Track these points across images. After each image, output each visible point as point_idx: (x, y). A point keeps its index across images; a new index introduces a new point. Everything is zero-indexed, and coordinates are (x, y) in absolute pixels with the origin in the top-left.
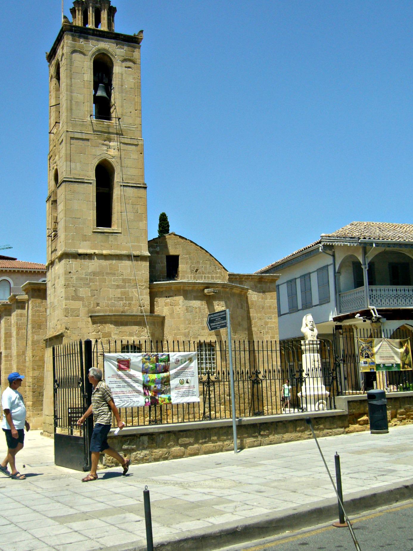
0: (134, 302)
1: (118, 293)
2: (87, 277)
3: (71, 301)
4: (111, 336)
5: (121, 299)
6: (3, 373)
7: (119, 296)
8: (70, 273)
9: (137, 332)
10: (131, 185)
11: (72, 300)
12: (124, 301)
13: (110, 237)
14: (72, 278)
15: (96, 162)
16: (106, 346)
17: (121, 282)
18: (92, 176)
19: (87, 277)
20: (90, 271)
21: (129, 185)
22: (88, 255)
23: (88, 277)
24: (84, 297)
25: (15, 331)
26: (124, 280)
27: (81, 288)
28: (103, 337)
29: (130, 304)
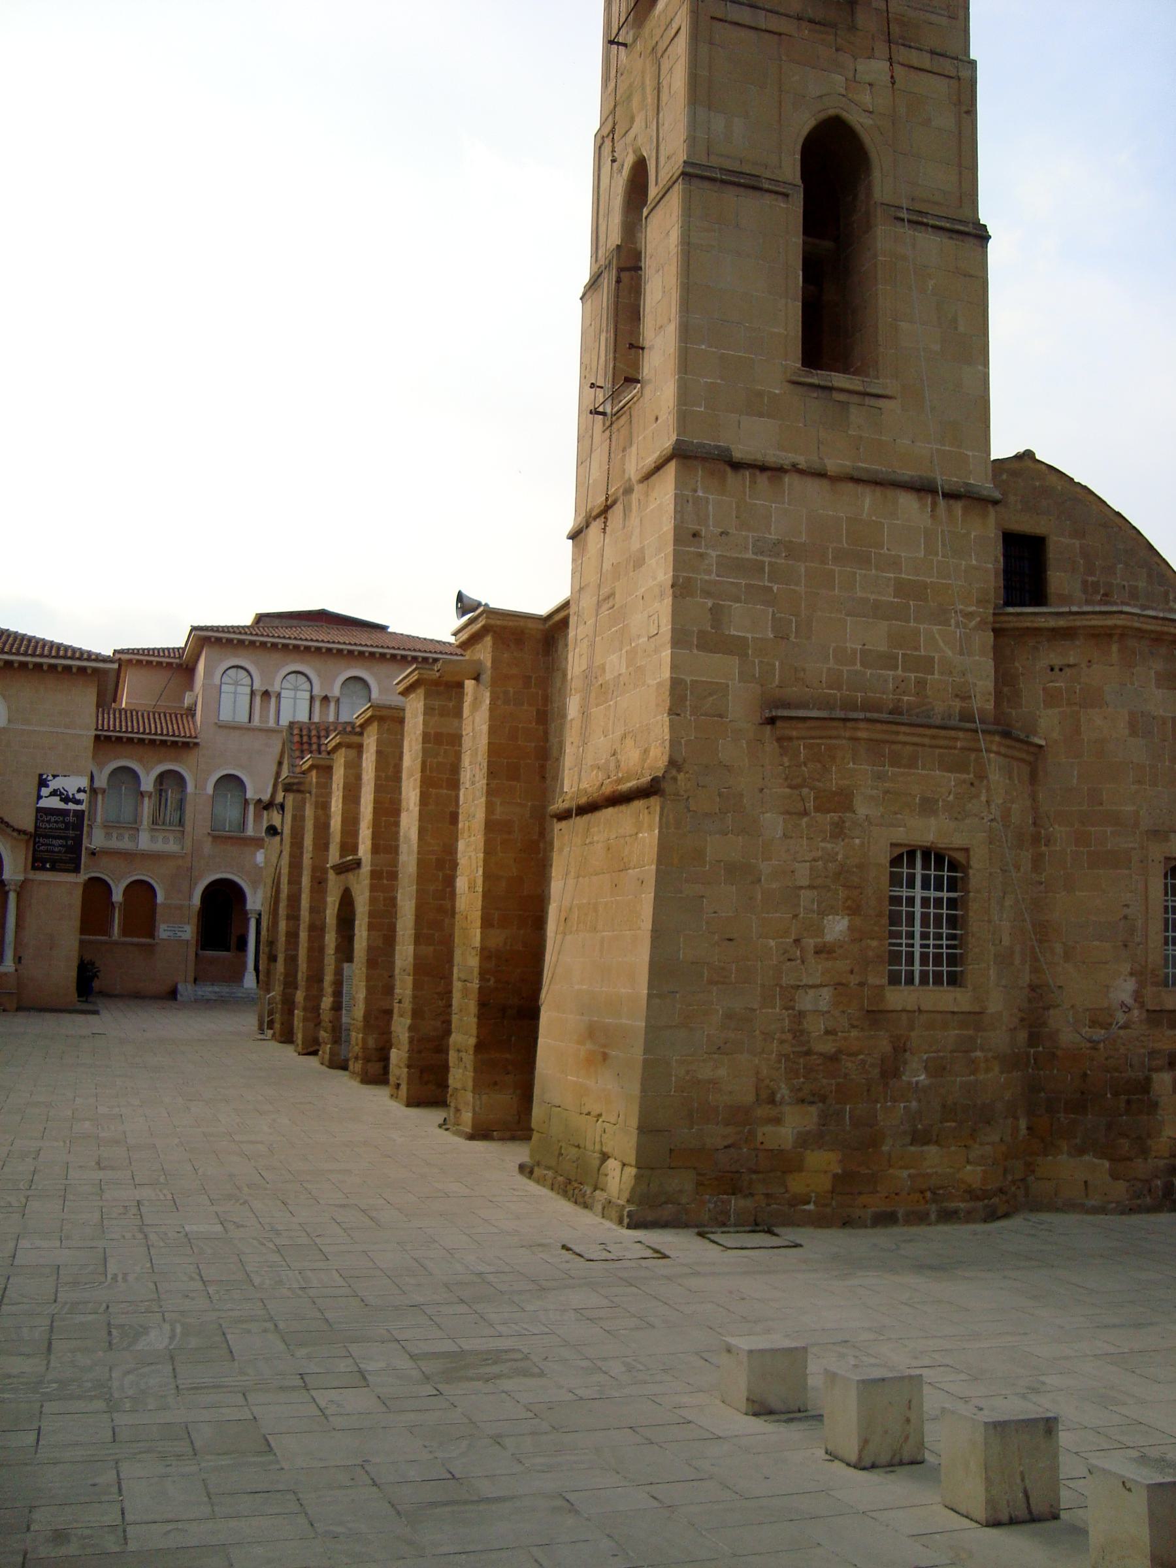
0: (936, 676)
1: (877, 636)
2: (760, 558)
3: (695, 651)
4: (850, 808)
5: (889, 661)
6: (365, 927)
7: (883, 648)
8: (695, 535)
9: (951, 798)
10: (931, 222)
11: (702, 647)
12: (900, 672)
13: (853, 410)
14: (701, 555)
15: (803, 123)
16: (829, 846)
17: (891, 590)
18: (790, 170)
19: (760, 558)
20: (773, 536)
21: (925, 220)
22: (769, 473)
23: (767, 559)
24: (748, 638)
25: (414, 790)
26: (901, 588)
27: (738, 600)
28: (817, 809)
29: (922, 684)
